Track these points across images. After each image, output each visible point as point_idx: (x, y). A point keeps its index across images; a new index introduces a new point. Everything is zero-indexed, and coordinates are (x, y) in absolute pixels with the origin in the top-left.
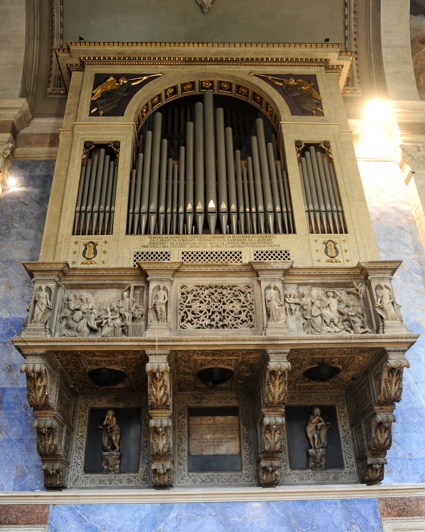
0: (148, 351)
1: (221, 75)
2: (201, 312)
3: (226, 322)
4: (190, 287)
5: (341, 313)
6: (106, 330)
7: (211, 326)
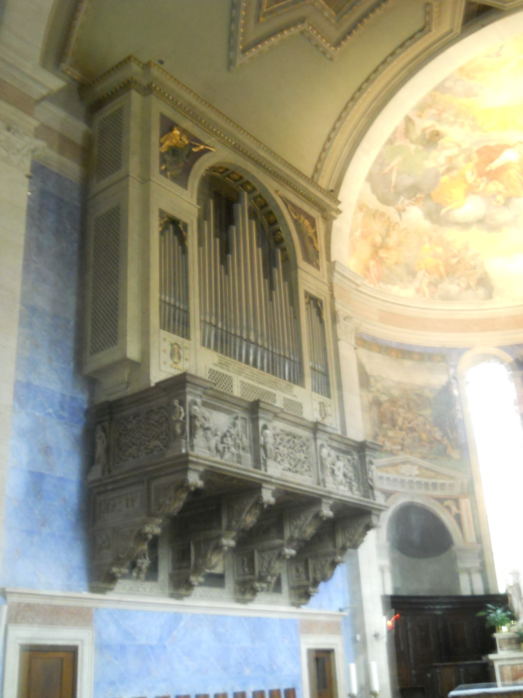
0: (264, 485)
1: (254, 177)
2: (284, 455)
3: (298, 468)
4: (278, 431)
5: (345, 475)
6: (227, 456)
7: (290, 470)
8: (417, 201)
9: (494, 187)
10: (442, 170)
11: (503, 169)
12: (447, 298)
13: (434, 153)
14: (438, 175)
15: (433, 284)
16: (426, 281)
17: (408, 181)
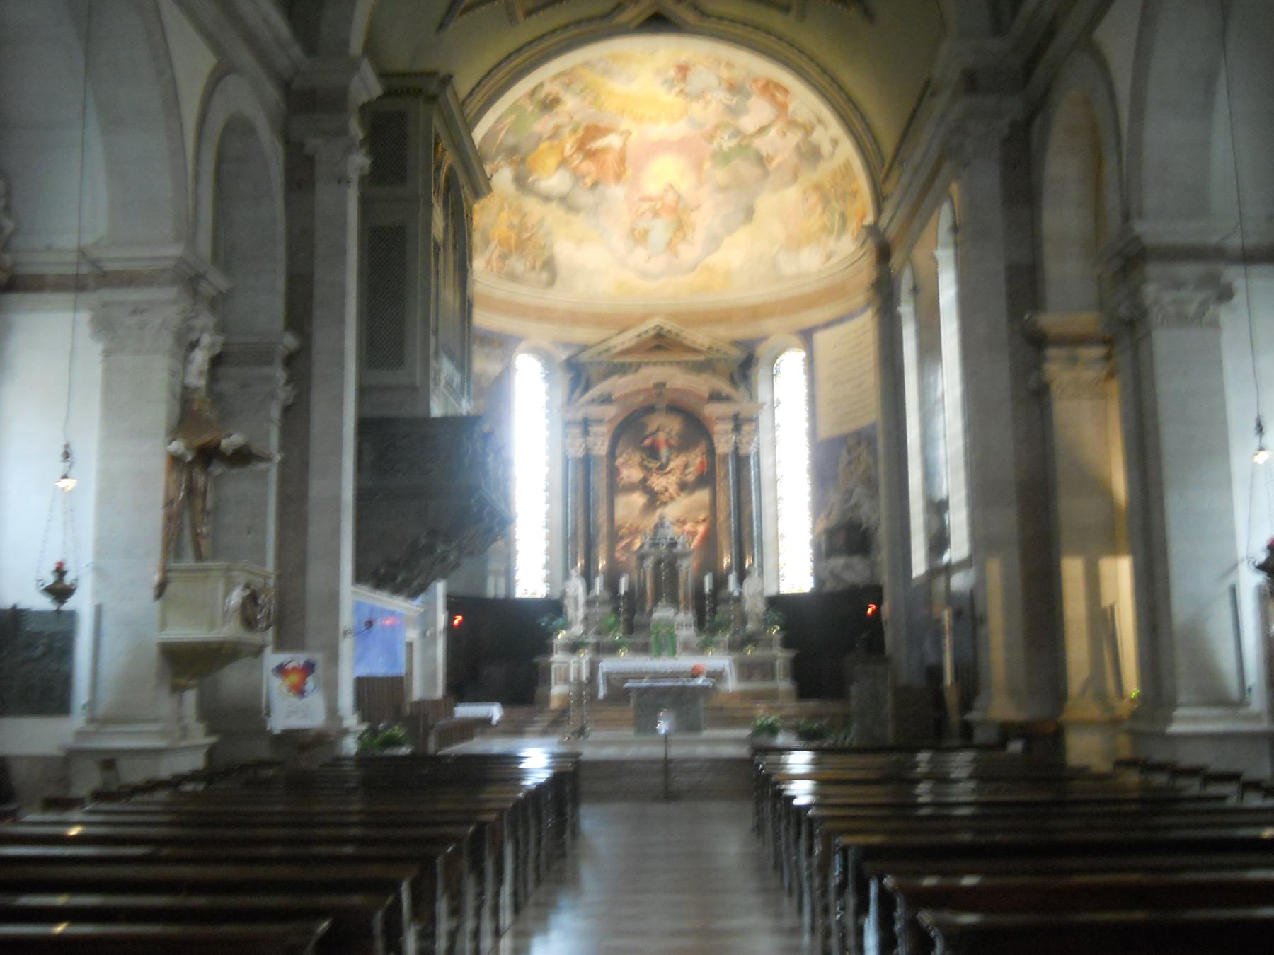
8: (511, 164)
9: (587, 166)
10: (546, 136)
11: (604, 151)
12: (513, 277)
13: (546, 117)
14: (540, 140)
15: (503, 258)
16: (496, 254)
17: (511, 141)
